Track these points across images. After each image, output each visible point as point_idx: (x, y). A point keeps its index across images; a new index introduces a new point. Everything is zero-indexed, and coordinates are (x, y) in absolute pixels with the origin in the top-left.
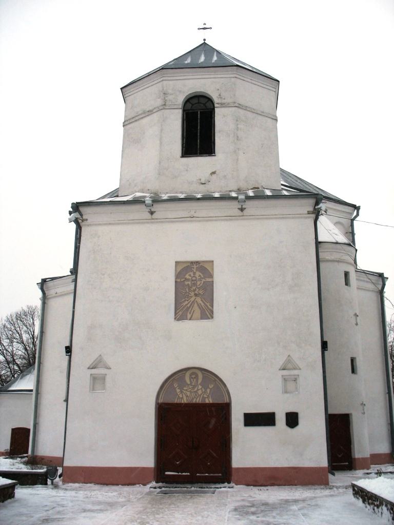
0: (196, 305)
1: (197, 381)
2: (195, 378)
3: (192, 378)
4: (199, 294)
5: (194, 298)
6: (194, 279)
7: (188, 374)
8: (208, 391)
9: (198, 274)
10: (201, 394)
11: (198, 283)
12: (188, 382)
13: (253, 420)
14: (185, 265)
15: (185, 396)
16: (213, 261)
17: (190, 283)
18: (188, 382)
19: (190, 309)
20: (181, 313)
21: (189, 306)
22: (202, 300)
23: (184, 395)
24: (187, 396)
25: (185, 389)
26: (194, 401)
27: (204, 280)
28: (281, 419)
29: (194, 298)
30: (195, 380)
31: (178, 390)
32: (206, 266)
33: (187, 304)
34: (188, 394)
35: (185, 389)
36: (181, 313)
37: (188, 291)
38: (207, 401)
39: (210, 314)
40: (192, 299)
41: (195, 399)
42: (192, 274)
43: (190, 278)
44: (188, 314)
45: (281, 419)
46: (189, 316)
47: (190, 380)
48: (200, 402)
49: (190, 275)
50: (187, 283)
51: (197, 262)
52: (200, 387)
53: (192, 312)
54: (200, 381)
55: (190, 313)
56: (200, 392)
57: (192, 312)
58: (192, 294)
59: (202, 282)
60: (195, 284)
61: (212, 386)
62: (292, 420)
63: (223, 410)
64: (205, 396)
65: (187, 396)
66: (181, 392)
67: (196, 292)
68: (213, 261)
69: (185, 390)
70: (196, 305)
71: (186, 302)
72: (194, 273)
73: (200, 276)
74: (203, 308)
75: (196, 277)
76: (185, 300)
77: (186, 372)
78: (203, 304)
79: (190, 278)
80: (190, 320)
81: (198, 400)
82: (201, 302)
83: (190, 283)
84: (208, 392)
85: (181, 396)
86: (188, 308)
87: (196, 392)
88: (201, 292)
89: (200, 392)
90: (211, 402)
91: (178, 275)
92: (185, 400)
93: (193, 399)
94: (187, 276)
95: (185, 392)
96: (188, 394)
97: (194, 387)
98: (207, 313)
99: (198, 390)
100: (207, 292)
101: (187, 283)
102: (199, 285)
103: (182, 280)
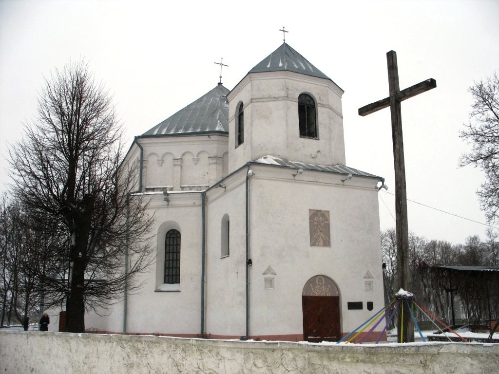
0: (320, 237)
7: (318, 277)
8: (328, 289)
9: (321, 218)
11: (321, 224)
12: (318, 284)
14: (314, 212)
15: (317, 292)
18: (318, 284)
20: (314, 242)
28: (365, 306)
31: (312, 289)
36: (314, 242)
38: (328, 295)
40: (319, 234)
45: (365, 306)
46: (317, 244)
50: (315, 223)
51: (320, 211)
56: (324, 290)
58: (318, 230)
60: (319, 224)
62: (370, 306)
63: (335, 301)
66: (314, 289)
70: (320, 237)
71: (315, 235)
72: (319, 218)
81: (323, 294)
88: (323, 229)
89: (324, 290)
90: (330, 295)
91: (311, 218)
92: (316, 295)
94: (315, 219)
98: (327, 243)
101: (315, 223)
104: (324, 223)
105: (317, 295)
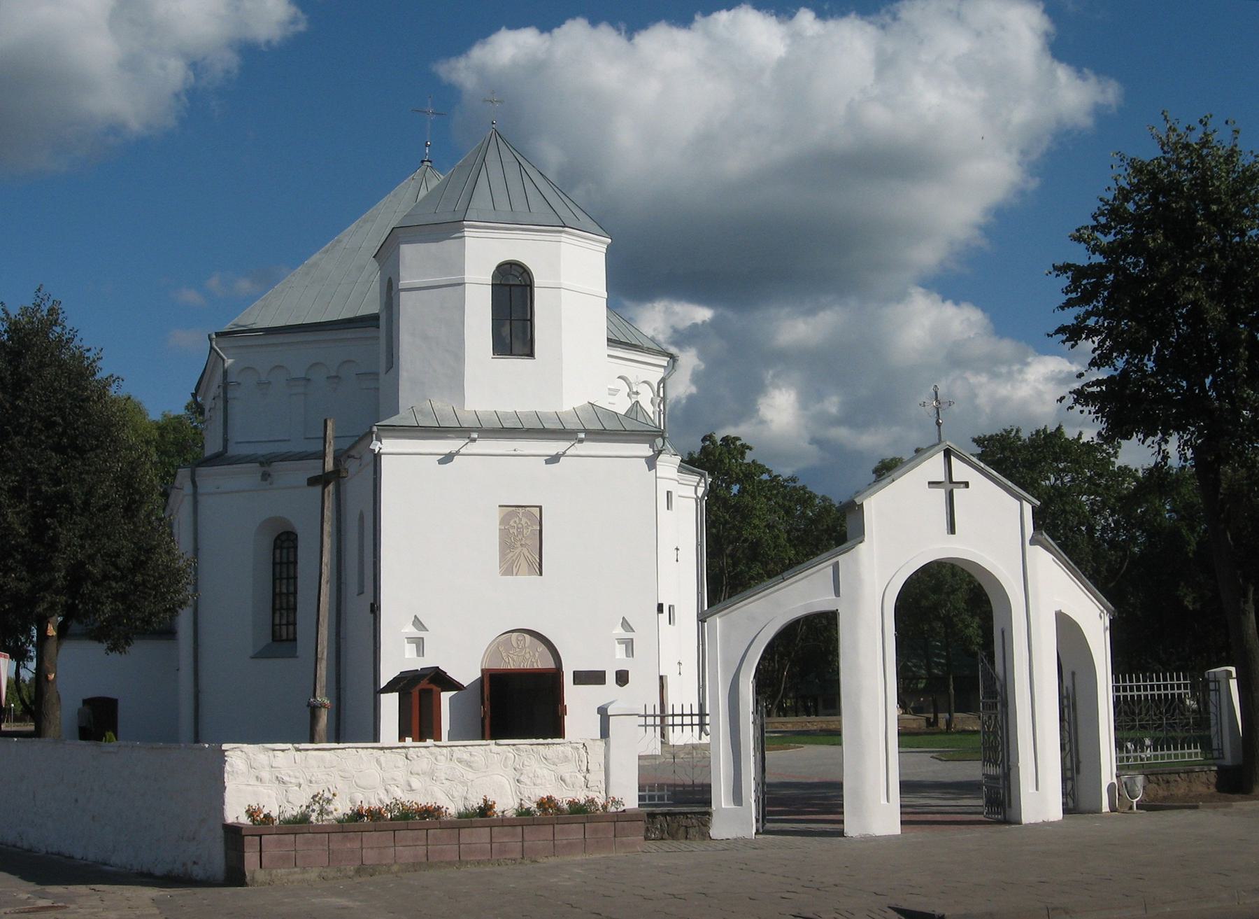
5: (520, 548)
8: (537, 654)
13: (583, 678)
18: (515, 645)
20: (508, 569)
21: (514, 558)
26: (522, 667)
28: (611, 678)
30: (522, 642)
33: (512, 557)
34: (515, 658)
38: (536, 667)
40: (518, 551)
43: (515, 525)
44: (514, 567)
45: (611, 678)
52: (528, 650)
55: (516, 567)
58: (519, 544)
62: (622, 678)
71: (511, 554)
72: (520, 520)
73: (526, 523)
75: (522, 524)
80: (516, 575)
85: (507, 661)
90: (540, 667)
91: (504, 521)
93: (520, 664)
97: (522, 649)
100: (508, 543)
104: (530, 528)
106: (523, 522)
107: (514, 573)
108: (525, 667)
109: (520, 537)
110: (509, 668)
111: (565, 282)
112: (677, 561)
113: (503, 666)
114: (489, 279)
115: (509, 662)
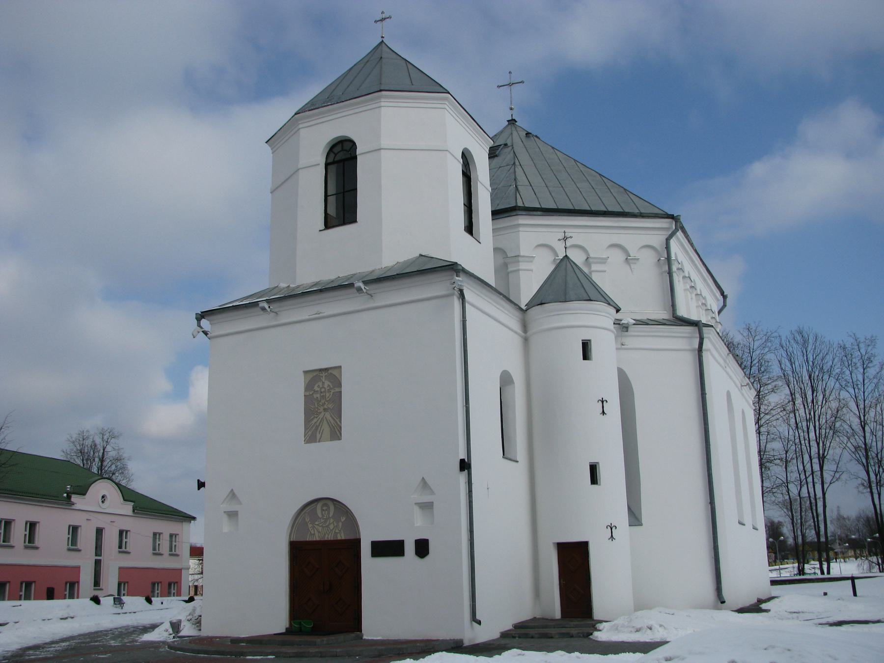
0: (325, 422)
1: (329, 513)
2: (326, 510)
3: (324, 510)
4: (329, 408)
6: (323, 390)
7: (319, 506)
8: (340, 524)
9: (327, 383)
10: (333, 529)
11: (327, 395)
12: (320, 515)
14: (314, 374)
15: (317, 533)
16: (340, 367)
17: (318, 396)
18: (320, 515)
19: (320, 426)
20: (311, 436)
21: (318, 424)
22: (331, 416)
23: (316, 530)
24: (319, 532)
25: (317, 523)
26: (326, 539)
27: (332, 391)
28: (410, 548)
29: (323, 413)
30: (326, 512)
31: (310, 526)
32: (335, 372)
34: (320, 529)
35: (317, 523)
36: (311, 436)
37: (316, 406)
38: (339, 538)
39: (338, 430)
40: (321, 416)
41: (327, 535)
42: (320, 384)
45: (410, 548)
46: (318, 436)
47: (322, 514)
48: (332, 539)
49: (319, 386)
50: (315, 396)
51: (326, 370)
52: (332, 520)
53: (321, 431)
54: (331, 514)
55: (319, 433)
56: (332, 527)
57: (321, 431)
58: (321, 409)
59: (331, 394)
60: (323, 397)
61: (344, 519)
62: (422, 548)
64: (337, 531)
65: (319, 532)
66: (313, 527)
67: (325, 407)
68: (340, 367)
69: (317, 525)
70: (325, 422)
71: (315, 420)
72: (323, 383)
73: (329, 386)
74: (332, 425)
75: (325, 389)
76: (314, 417)
77: (317, 504)
78: (332, 421)
79: (319, 389)
80: (319, 442)
81: (330, 537)
82: (330, 418)
83: (318, 396)
84: (340, 526)
86: (317, 427)
87: (328, 526)
88: (330, 406)
89: (332, 527)
90: (343, 538)
91: (309, 387)
92: (317, 538)
93: (325, 535)
94: (316, 388)
95: (316, 526)
96: (320, 529)
97: (326, 520)
98: (336, 434)
99: (330, 524)
101: (315, 396)
102: (329, 397)
103: (311, 393)
104: (332, 391)
105: (318, 539)
106: (326, 386)
107: (317, 441)
108: (330, 539)
109: (323, 401)
110: (314, 539)
111: (384, 143)
112: (603, 413)
113: (309, 538)
114: (322, 161)
115: (314, 534)
